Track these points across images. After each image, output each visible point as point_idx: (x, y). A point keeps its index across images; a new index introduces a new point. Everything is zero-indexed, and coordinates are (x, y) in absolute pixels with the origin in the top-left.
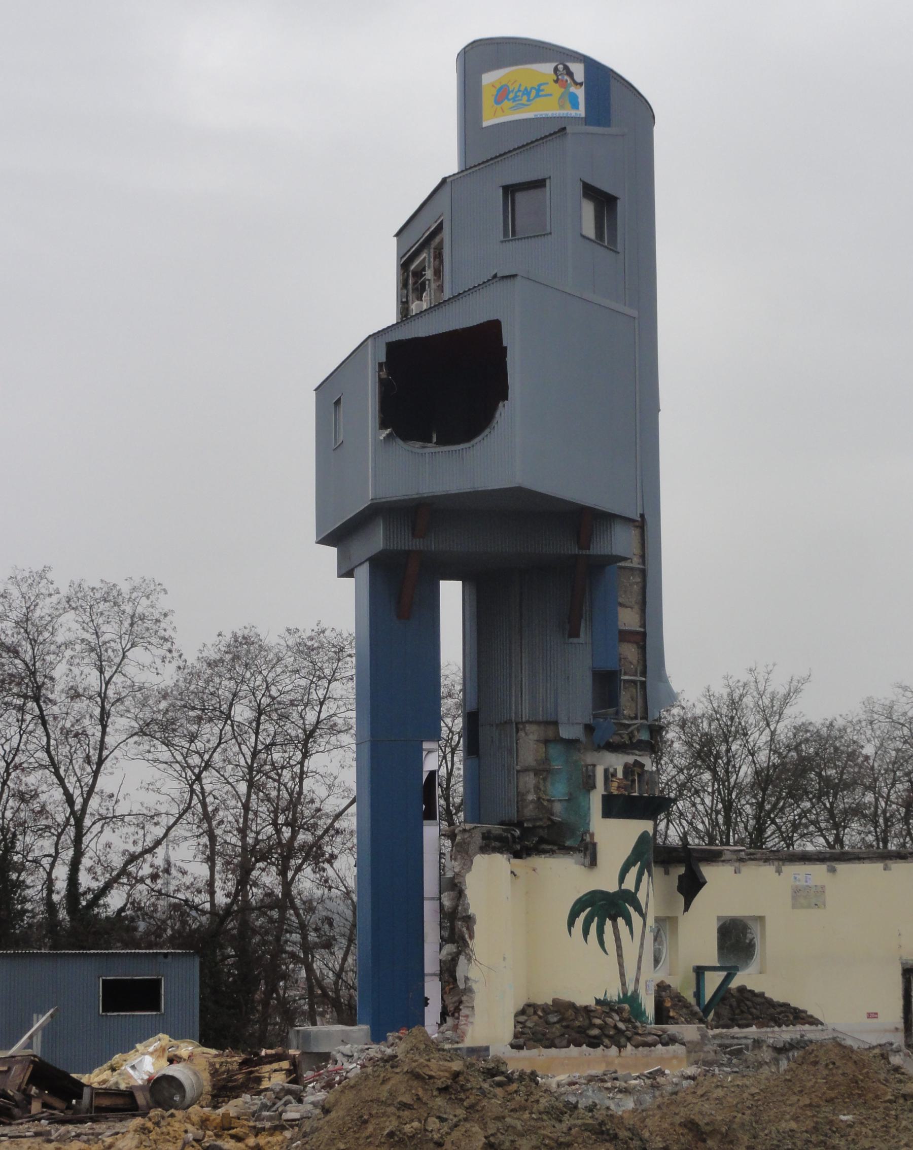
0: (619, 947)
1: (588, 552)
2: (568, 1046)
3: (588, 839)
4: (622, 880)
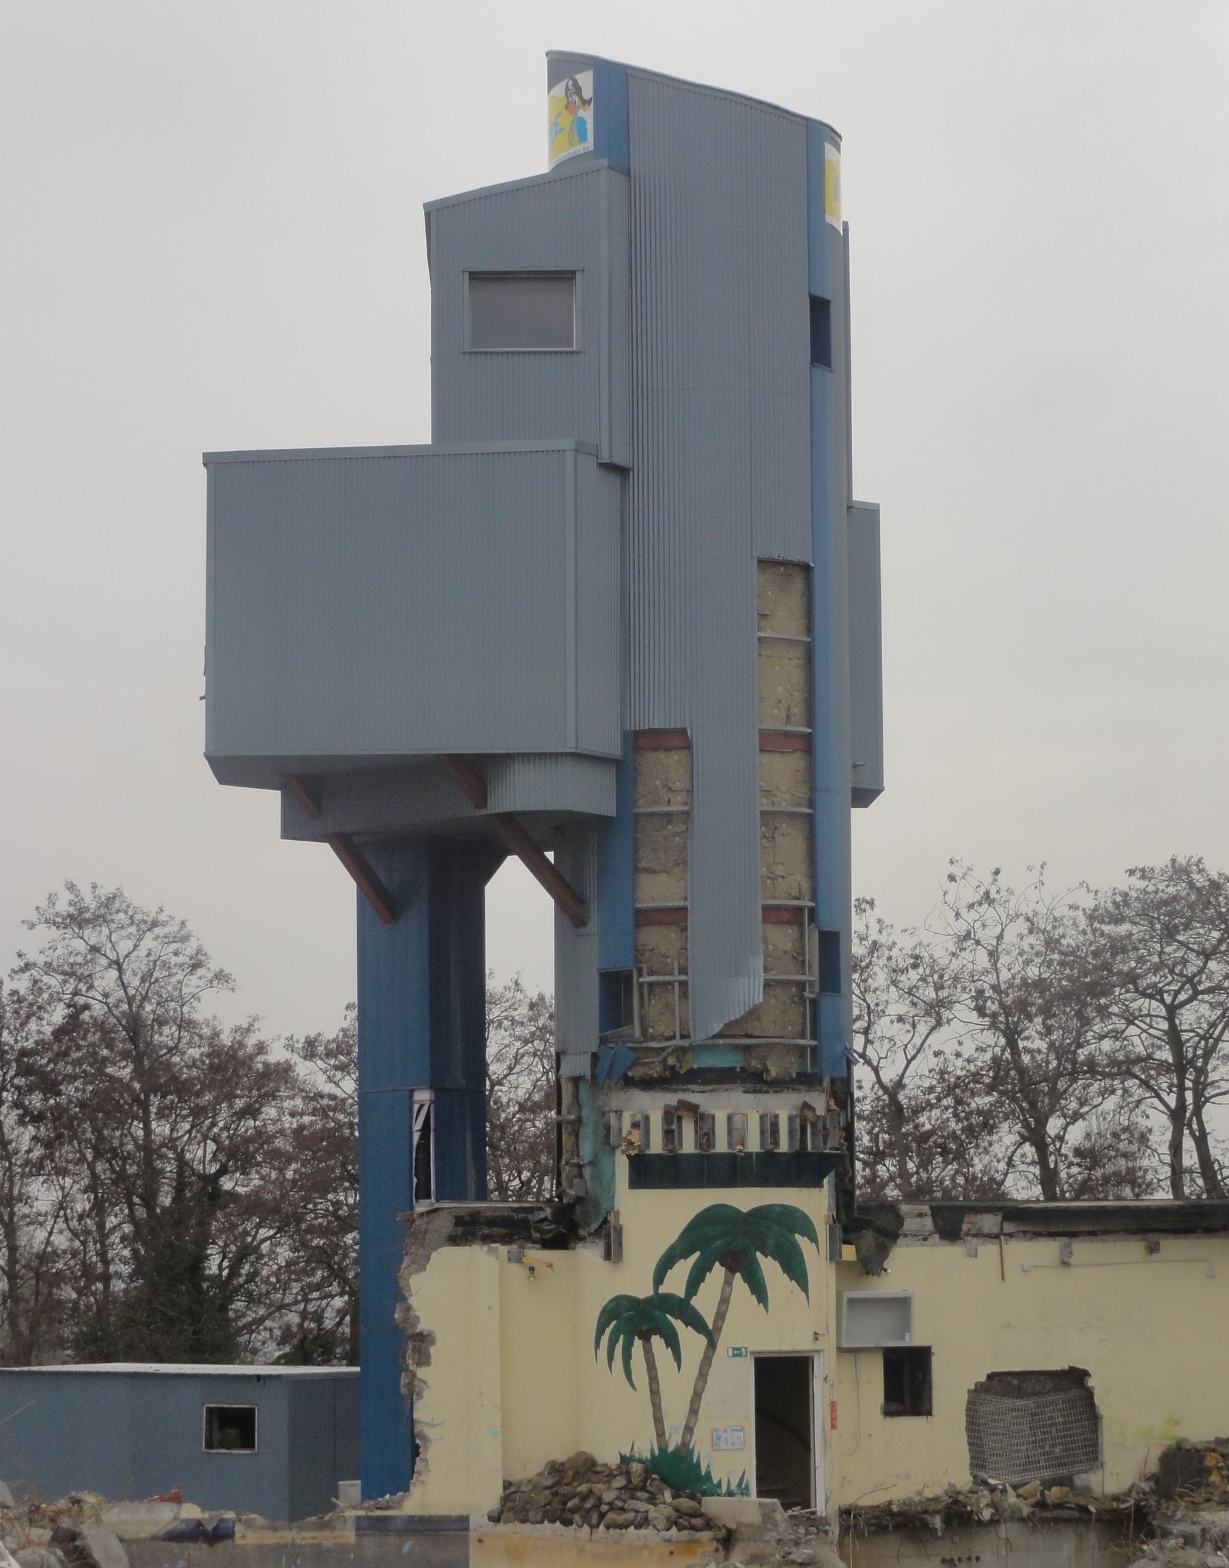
1: (484, 812)
2: (542, 1522)
3: (611, 1219)
4: (659, 1278)
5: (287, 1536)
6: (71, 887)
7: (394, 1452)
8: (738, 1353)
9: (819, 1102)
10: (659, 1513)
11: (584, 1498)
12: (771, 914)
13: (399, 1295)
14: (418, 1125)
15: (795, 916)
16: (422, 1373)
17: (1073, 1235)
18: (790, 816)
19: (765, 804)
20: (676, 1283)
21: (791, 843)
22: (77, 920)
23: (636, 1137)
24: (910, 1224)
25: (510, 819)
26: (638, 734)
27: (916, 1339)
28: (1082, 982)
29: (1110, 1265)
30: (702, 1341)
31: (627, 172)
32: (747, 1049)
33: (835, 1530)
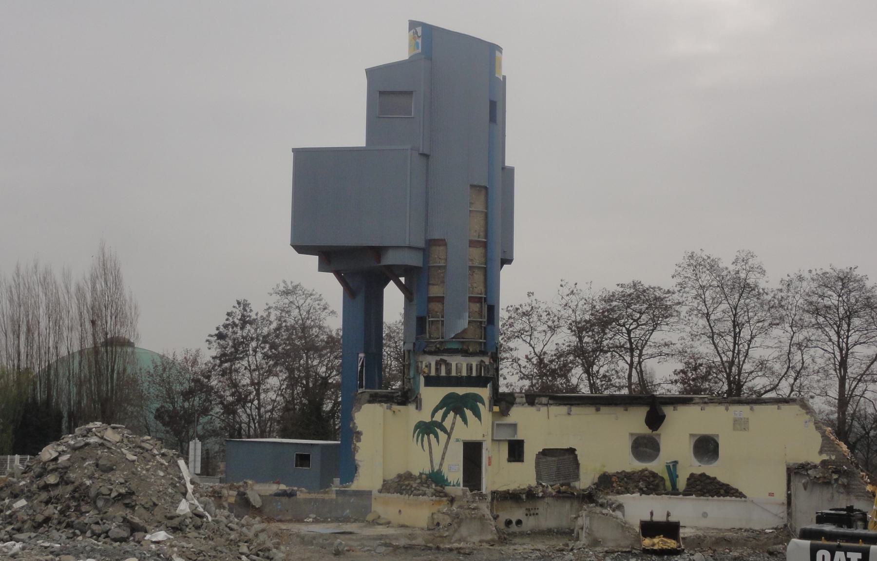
0: (430, 448)
4: (433, 416)
5: (313, 496)
6: (284, 282)
7: (350, 470)
8: (457, 440)
9: (487, 360)
10: (429, 491)
11: (407, 486)
12: (472, 299)
13: (352, 419)
14: (360, 364)
15: (478, 300)
16: (358, 444)
17: (572, 405)
18: (479, 268)
19: (470, 264)
20: (438, 417)
21: (479, 276)
22: (286, 293)
23: (426, 370)
24: (518, 400)
25: (389, 267)
26: (431, 240)
27: (519, 437)
28: (603, 320)
29: (584, 416)
30: (446, 436)
31: (431, 60)
32: (463, 343)
33: (489, 498)
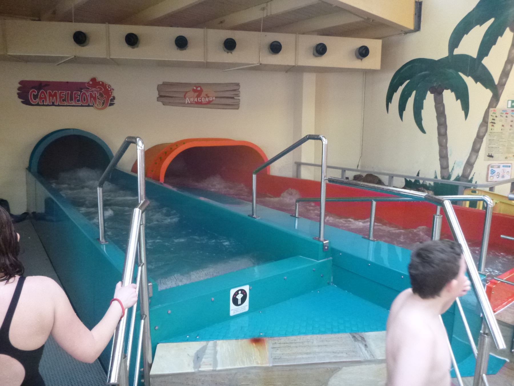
30: (488, 94)
